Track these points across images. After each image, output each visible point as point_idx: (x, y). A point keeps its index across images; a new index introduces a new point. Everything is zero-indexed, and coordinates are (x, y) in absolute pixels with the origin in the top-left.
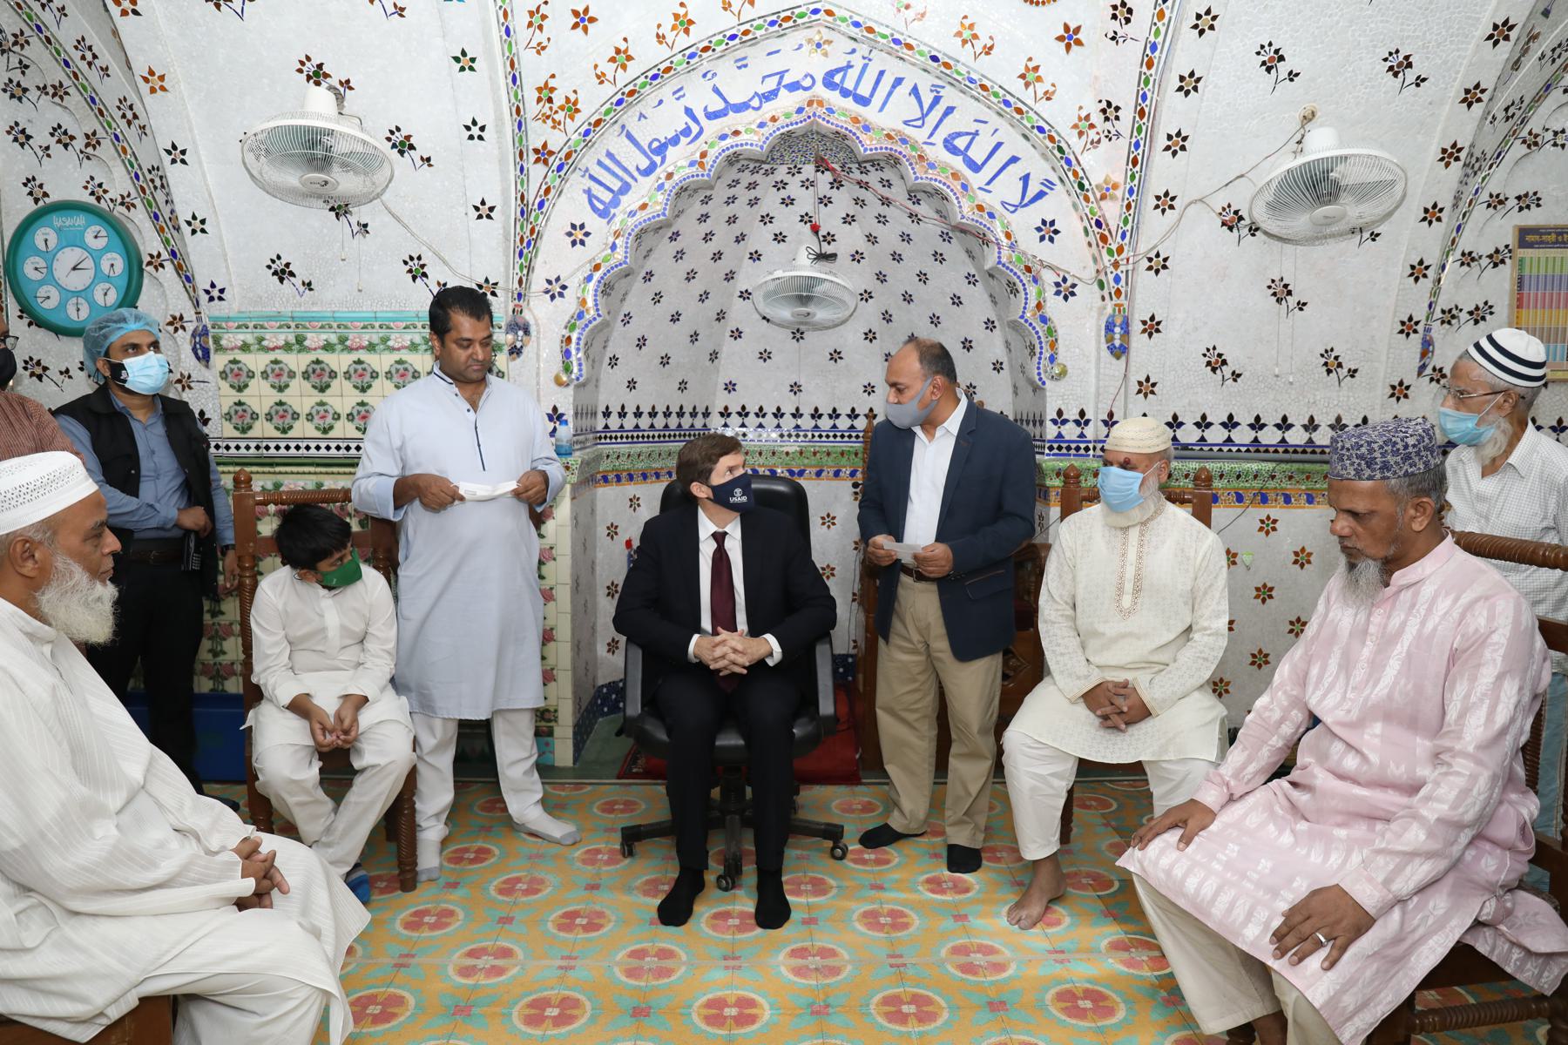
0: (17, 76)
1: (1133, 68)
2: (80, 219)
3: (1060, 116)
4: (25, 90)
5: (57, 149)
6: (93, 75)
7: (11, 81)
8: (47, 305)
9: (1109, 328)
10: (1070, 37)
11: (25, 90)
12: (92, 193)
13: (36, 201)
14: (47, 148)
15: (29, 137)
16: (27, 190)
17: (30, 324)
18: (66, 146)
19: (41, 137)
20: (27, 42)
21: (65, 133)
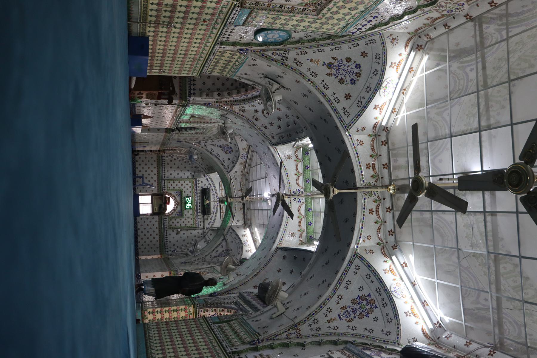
1: (248, 117)
3: (246, 106)
6: (315, 49)
9: (209, 104)
10: (256, 111)
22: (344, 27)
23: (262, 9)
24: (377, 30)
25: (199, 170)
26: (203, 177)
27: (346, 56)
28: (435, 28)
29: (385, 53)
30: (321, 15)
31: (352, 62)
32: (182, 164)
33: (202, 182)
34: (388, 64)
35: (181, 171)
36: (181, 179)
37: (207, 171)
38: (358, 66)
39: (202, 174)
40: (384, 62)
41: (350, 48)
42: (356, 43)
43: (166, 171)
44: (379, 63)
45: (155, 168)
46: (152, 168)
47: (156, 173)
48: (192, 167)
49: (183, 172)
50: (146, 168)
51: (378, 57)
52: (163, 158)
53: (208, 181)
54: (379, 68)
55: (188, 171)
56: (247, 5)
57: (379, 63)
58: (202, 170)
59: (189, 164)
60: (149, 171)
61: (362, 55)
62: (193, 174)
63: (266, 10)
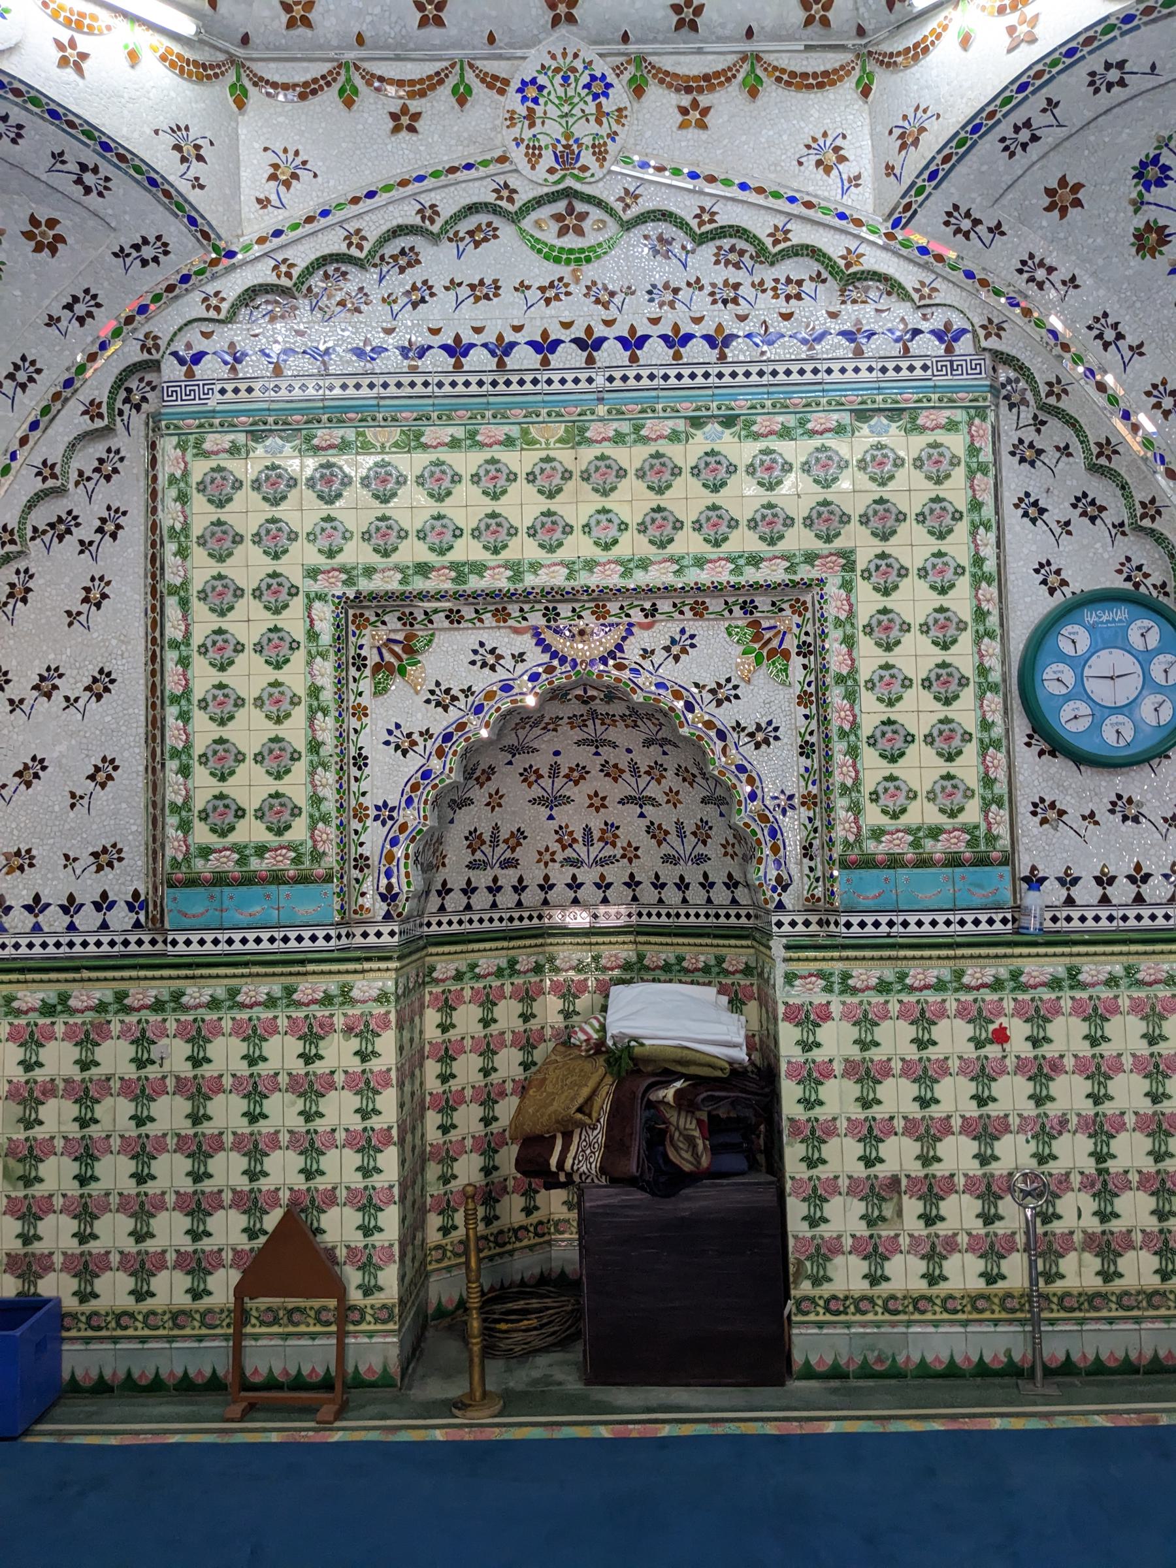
0: (1029, 435)
2: (1121, 613)
4: (1040, 452)
5: (1080, 525)
7: (1021, 441)
8: (1073, 727)
11: (1040, 452)
12: (1128, 579)
13: (1052, 591)
14: (1067, 523)
15: (1042, 511)
16: (1040, 577)
17: (1041, 753)
18: (1093, 519)
19: (1059, 509)
20: (1065, 392)
21: (1093, 503)
22: (894, 413)
23: (830, 826)
24: (875, 260)
27: (1135, 262)
28: (750, 33)
29: (976, 127)
30: (805, 572)
31: (1150, 214)
34: (1028, 56)
38: (1152, 172)
40: (1022, 88)
41: (1072, 282)
42: (1020, 281)
44: (1051, 104)
51: (1024, 135)
54: (1071, 86)
56: (819, 892)
57: (1051, 104)
61: (1077, 203)
63: (829, 809)
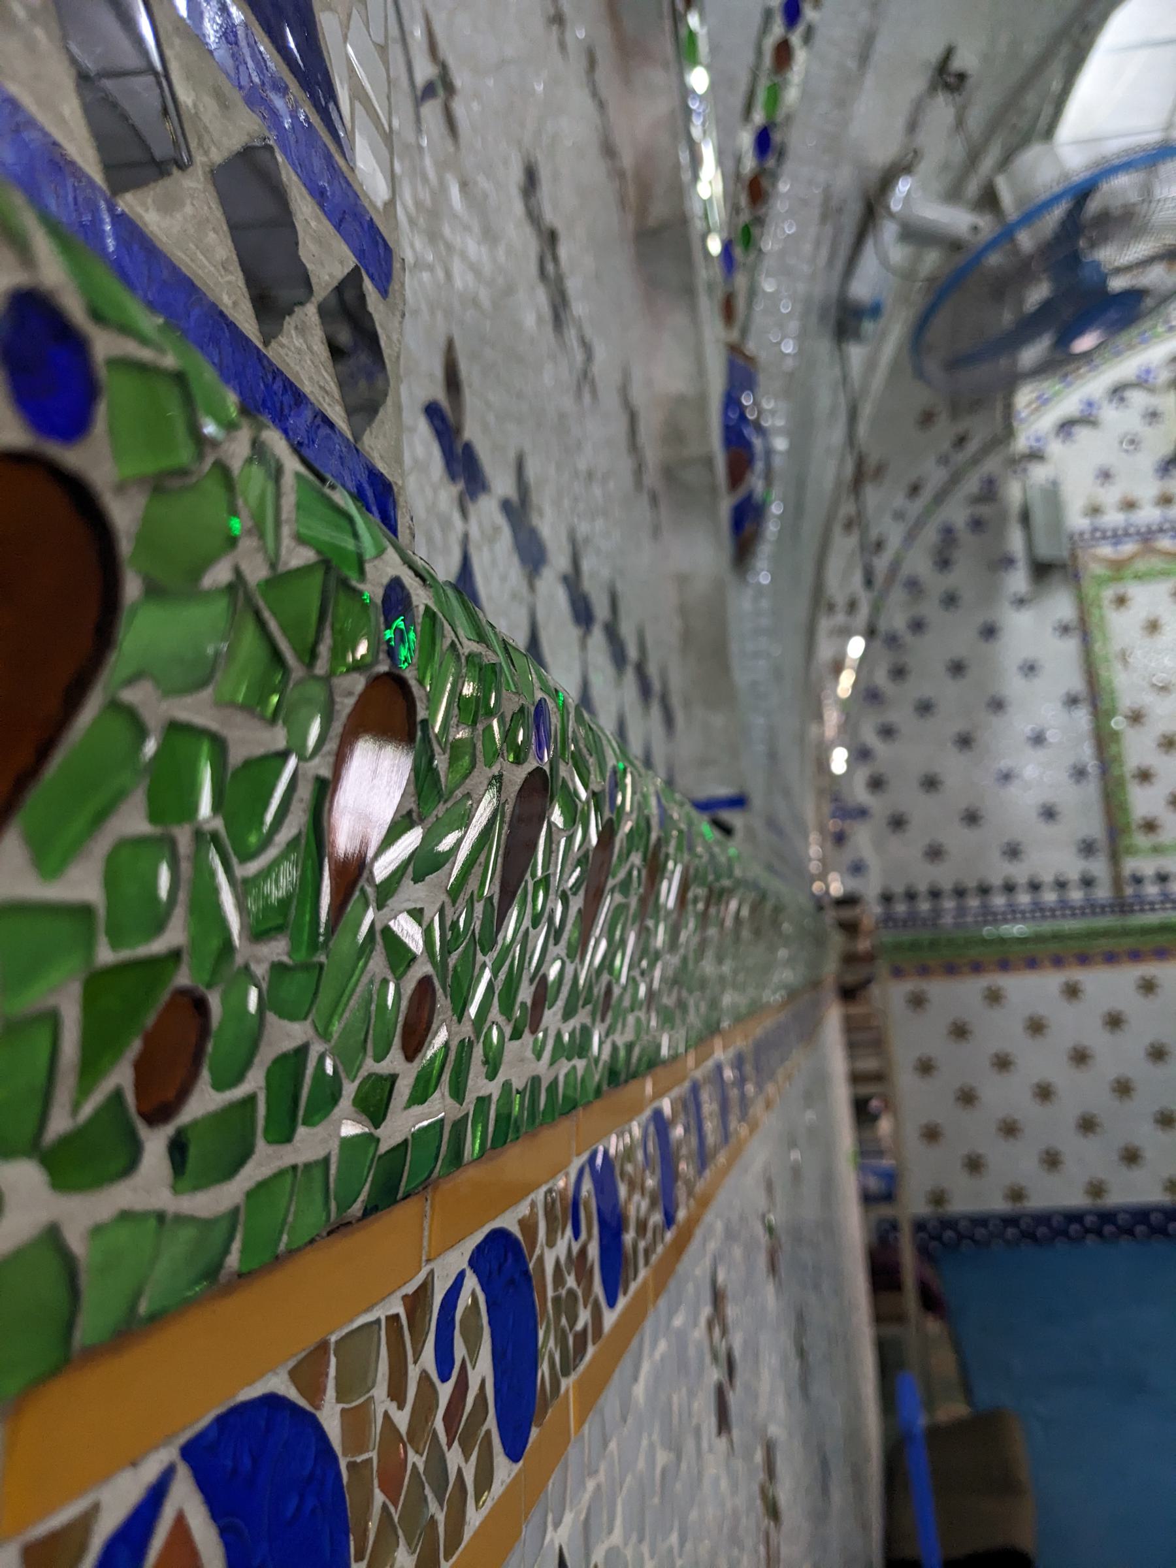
25: (977, 524)
26: (1039, 473)
32: (925, 708)
33: (1105, 476)
35: (997, 705)
36: (1094, 695)
37: (980, 429)
39: (1014, 493)
43: (1020, 872)
45: (994, 997)
46: (1001, 1030)
47: (1050, 981)
48: (950, 600)
49: (1014, 686)
50: (1005, 1095)
52: (872, 910)
53: (1087, 419)
55: (990, 632)
58: (972, 484)
59: (917, 626)
60: (1041, 1061)
62: (1018, 580)
